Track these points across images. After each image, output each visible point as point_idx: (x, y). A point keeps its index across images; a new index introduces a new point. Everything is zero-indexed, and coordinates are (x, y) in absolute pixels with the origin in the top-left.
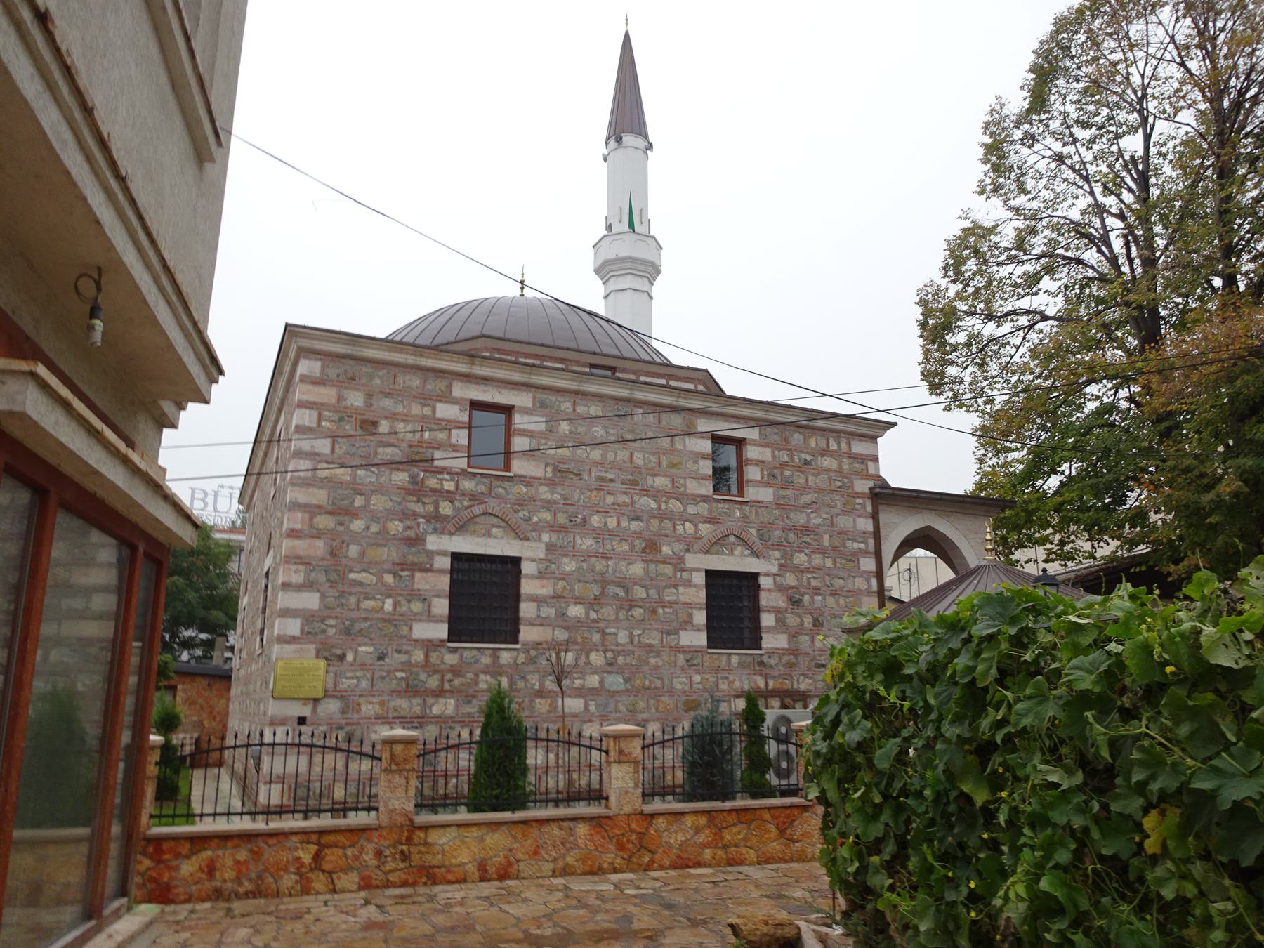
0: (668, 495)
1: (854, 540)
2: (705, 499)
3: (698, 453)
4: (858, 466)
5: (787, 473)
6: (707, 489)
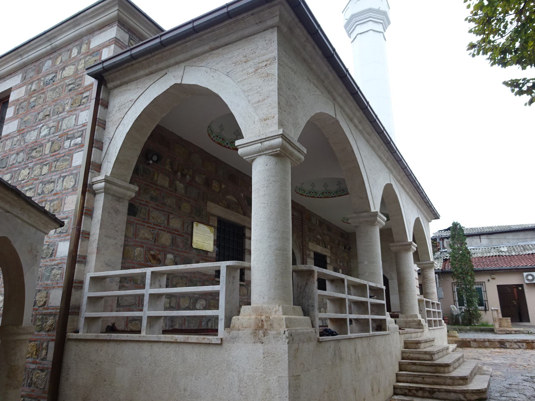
1: (73, 137)
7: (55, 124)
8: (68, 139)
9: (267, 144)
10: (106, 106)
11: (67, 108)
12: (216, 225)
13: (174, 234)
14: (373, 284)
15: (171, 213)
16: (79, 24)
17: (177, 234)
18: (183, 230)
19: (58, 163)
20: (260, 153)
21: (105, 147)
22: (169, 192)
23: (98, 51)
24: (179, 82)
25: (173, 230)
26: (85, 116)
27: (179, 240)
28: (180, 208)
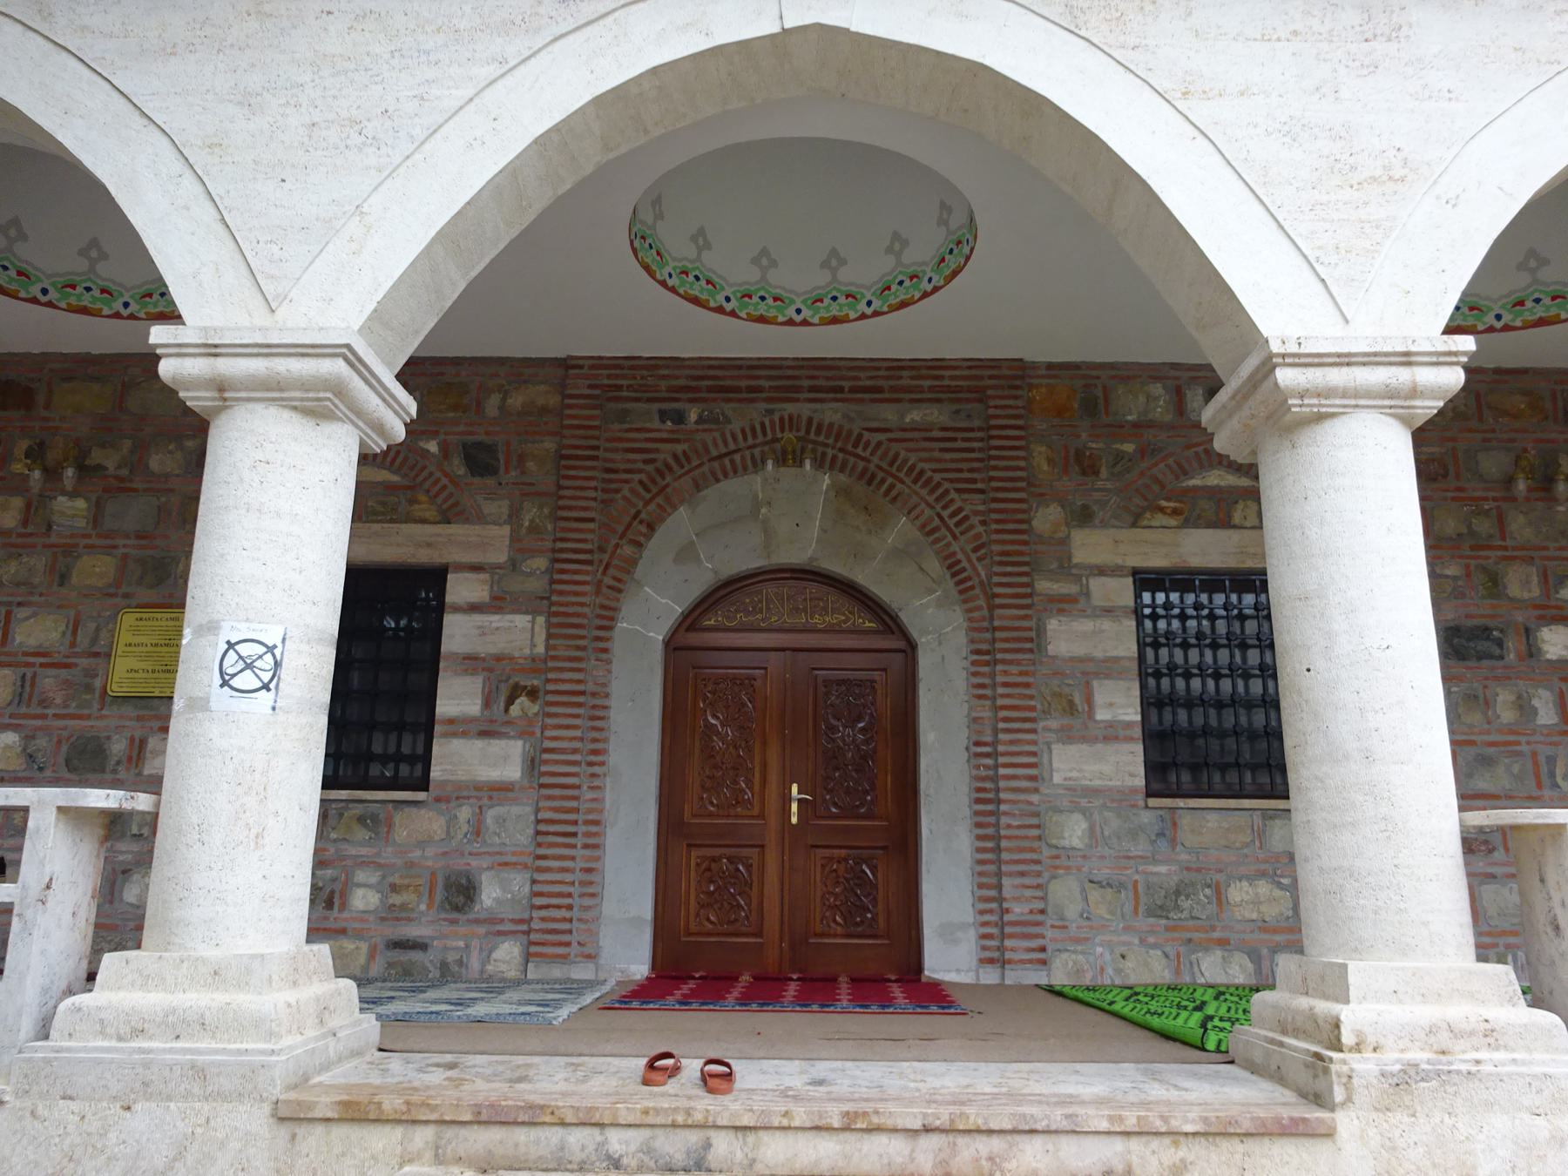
13: (28, 665)
15: (19, 604)
17: (42, 665)
18: (73, 644)
22: (20, 540)
25: (26, 654)
27: (49, 681)
28: (63, 579)
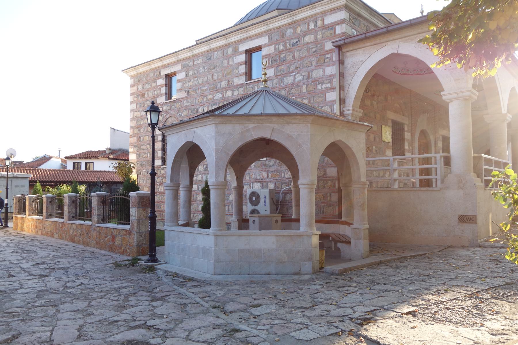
0: (226, 89)
1: (323, 83)
2: (241, 85)
3: (239, 63)
4: (328, 33)
5: (283, 56)
6: (242, 80)
7: (307, 73)
8: (319, 84)
9: (460, 95)
10: (343, 64)
11: (314, 64)
12: (391, 125)
14: (504, 161)
16: (315, 8)
19: (315, 99)
20: (456, 99)
21: (346, 89)
23: (332, 26)
24: (396, 52)
26: (332, 70)
